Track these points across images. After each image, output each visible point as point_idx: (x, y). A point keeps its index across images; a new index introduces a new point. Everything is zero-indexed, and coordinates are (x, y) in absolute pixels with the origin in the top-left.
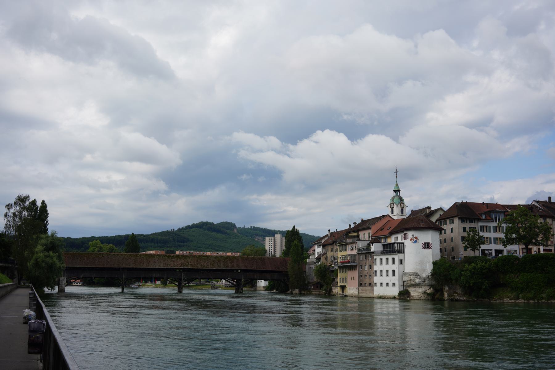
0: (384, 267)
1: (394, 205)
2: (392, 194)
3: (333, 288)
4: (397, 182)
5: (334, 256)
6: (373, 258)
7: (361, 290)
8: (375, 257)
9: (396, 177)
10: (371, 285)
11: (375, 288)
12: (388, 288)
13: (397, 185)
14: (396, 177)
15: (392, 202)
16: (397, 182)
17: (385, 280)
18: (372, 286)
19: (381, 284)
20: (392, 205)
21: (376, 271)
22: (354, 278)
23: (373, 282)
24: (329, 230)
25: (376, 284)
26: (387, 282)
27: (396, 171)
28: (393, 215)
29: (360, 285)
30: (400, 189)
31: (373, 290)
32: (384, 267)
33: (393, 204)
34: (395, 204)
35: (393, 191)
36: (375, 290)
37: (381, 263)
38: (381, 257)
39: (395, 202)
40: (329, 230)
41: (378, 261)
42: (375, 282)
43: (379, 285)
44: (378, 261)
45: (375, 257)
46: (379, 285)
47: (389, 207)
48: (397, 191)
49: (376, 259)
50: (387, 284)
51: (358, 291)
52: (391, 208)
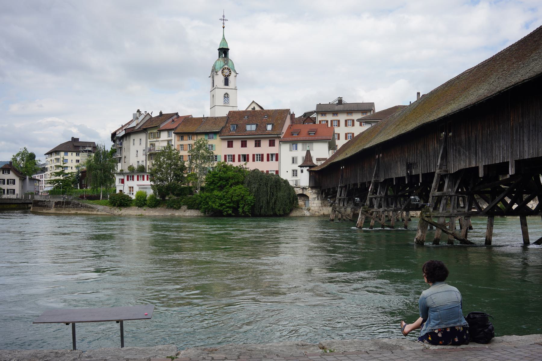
1: (230, 71)
4: (224, 35)
9: (224, 27)
13: (224, 38)
14: (224, 27)
15: (226, 66)
16: (224, 35)
20: (226, 71)
27: (224, 16)
28: (227, 87)
30: (229, 48)
33: (229, 69)
34: (232, 71)
35: (219, 49)
39: (230, 66)
47: (220, 73)
52: (223, 75)
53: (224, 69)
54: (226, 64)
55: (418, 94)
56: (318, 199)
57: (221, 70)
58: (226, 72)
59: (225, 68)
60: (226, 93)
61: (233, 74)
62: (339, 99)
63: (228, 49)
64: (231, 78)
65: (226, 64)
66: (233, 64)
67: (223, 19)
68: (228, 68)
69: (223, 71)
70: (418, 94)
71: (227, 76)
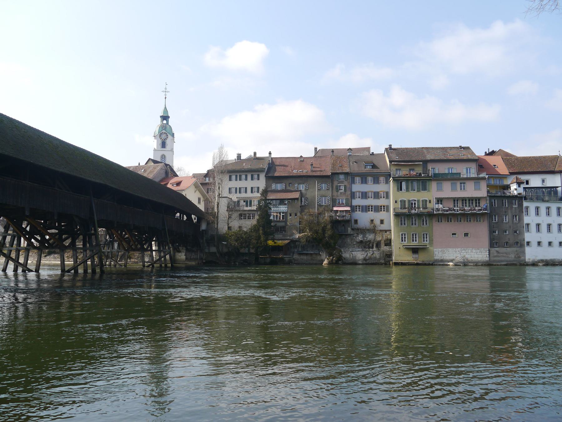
0: (544, 220)
1: (167, 135)
2: (158, 121)
3: (342, 250)
4: (165, 105)
5: (334, 198)
6: (521, 205)
7: (495, 252)
8: (525, 204)
9: (166, 98)
10: (521, 244)
11: (527, 249)
12: (550, 249)
13: (165, 108)
14: (166, 98)
15: (164, 131)
16: (165, 105)
17: (545, 237)
18: (522, 246)
19: (539, 243)
21: (528, 225)
22: (466, 235)
23: (524, 240)
24: (270, 153)
25: (528, 243)
26: (550, 241)
27: (166, 89)
29: (493, 243)
31: (524, 252)
32: (544, 220)
33: (166, 134)
35: (161, 117)
36: (526, 252)
37: (537, 214)
38: (548, 205)
39: (168, 131)
40: (270, 153)
41: (532, 211)
42: (527, 240)
43: (534, 244)
44: (532, 211)
45: (525, 204)
46: (534, 244)
48: (165, 117)
49: (527, 208)
50: (550, 244)
51: (488, 254)
53: (161, 134)
54: (164, 129)
55: (316, 149)
56: (155, 246)
57: (159, 135)
58: (164, 136)
59: (163, 133)
60: (163, 155)
61: (170, 137)
62: (238, 155)
63: (169, 117)
64: (168, 142)
65: (165, 129)
66: (171, 129)
67: (165, 91)
68: (165, 133)
69: (160, 135)
70: (316, 149)
71: (164, 139)
